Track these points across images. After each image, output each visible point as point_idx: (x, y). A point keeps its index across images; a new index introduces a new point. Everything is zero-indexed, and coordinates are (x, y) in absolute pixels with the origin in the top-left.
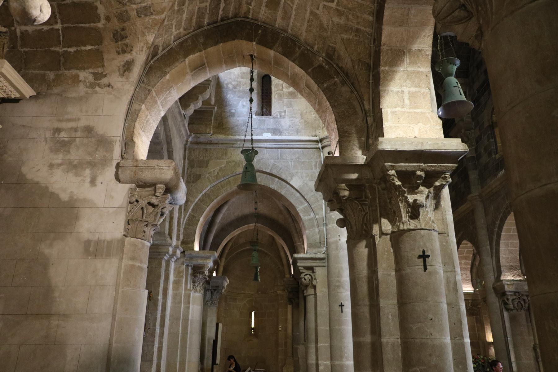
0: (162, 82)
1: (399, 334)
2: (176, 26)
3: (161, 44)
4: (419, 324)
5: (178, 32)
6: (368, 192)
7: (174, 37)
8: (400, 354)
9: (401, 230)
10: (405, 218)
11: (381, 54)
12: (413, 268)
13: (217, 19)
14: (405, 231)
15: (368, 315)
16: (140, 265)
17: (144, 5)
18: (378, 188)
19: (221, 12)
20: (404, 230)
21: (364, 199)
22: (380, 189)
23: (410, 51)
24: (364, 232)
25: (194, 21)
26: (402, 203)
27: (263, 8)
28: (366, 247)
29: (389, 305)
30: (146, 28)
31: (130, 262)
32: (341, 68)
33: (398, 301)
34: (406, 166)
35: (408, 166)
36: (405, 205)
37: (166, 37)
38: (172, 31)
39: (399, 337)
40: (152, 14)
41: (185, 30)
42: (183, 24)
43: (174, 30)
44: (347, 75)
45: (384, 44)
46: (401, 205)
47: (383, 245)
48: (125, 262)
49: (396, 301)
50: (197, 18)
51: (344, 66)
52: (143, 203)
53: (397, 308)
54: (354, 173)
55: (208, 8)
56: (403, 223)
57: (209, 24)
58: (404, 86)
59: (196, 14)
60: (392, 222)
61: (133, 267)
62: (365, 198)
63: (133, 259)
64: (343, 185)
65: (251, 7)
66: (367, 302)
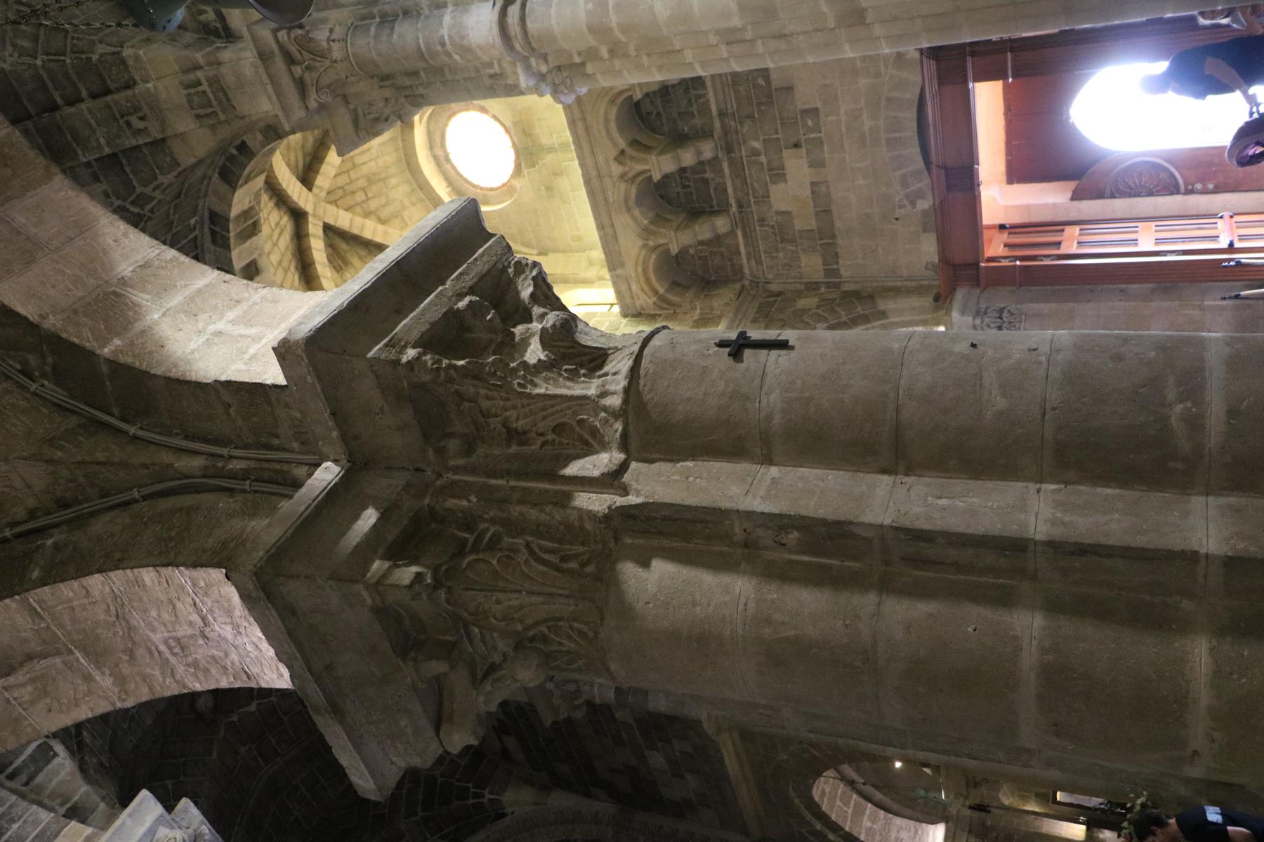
1: (1020, 485)
4: (987, 382)
6: (451, 503)
8: (1109, 491)
9: (626, 401)
10: (590, 388)
11: (64, 335)
12: (769, 380)
14: (630, 391)
15: (922, 608)
18: (456, 470)
20: (627, 391)
21: (471, 538)
22: (460, 462)
23: (123, 282)
24: (590, 569)
26: (536, 385)
28: (646, 564)
29: (888, 500)
32: (32, 514)
33: (884, 471)
34: (418, 318)
36: (547, 380)
39: (1033, 487)
44: (63, 504)
45: (43, 317)
46: (541, 391)
47: (655, 483)
49: (886, 479)
51: (32, 502)
53: (909, 480)
54: (357, 517)
56: (604, 394)
58: (205, 328)
60: (589, 444)
62: (469, 527)
64: (378, 566)
66: (867, 601)
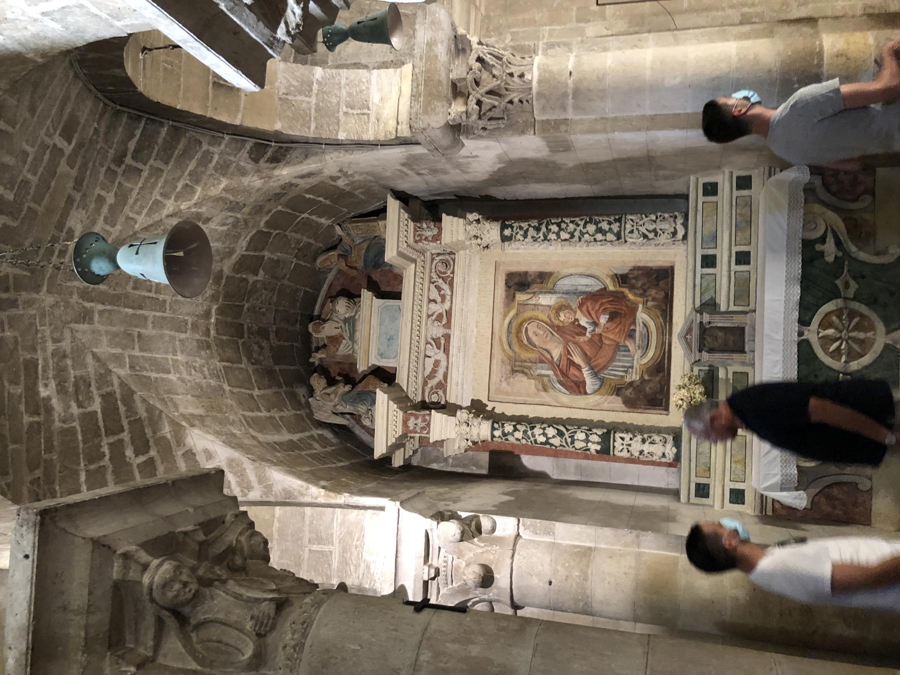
0: (290, 128)
2: (210, 162)
3: (244, 154)
5: (212, 149)
7: (219, 145)
13: (146, 124)
16: (570, 97)
17: (230, 214)
19: (138, 133)
25: (181, 146)
27: (82, 121)
30: (250, 193)
31: (570, 110)
35: (249, 25)
37: (232, 158)
38: (219, 158)
40: (231, 202)
41: (200, 143)
42: (198, 156)
43: (216, 157)
48: (570, 115)
50: (176, 148)
52: (481, 123)
55: (153, 157)
57: (162, 125)
59: (175, 156)
61: (575, 107)
63: (564, 108)
65: (95, 125)
